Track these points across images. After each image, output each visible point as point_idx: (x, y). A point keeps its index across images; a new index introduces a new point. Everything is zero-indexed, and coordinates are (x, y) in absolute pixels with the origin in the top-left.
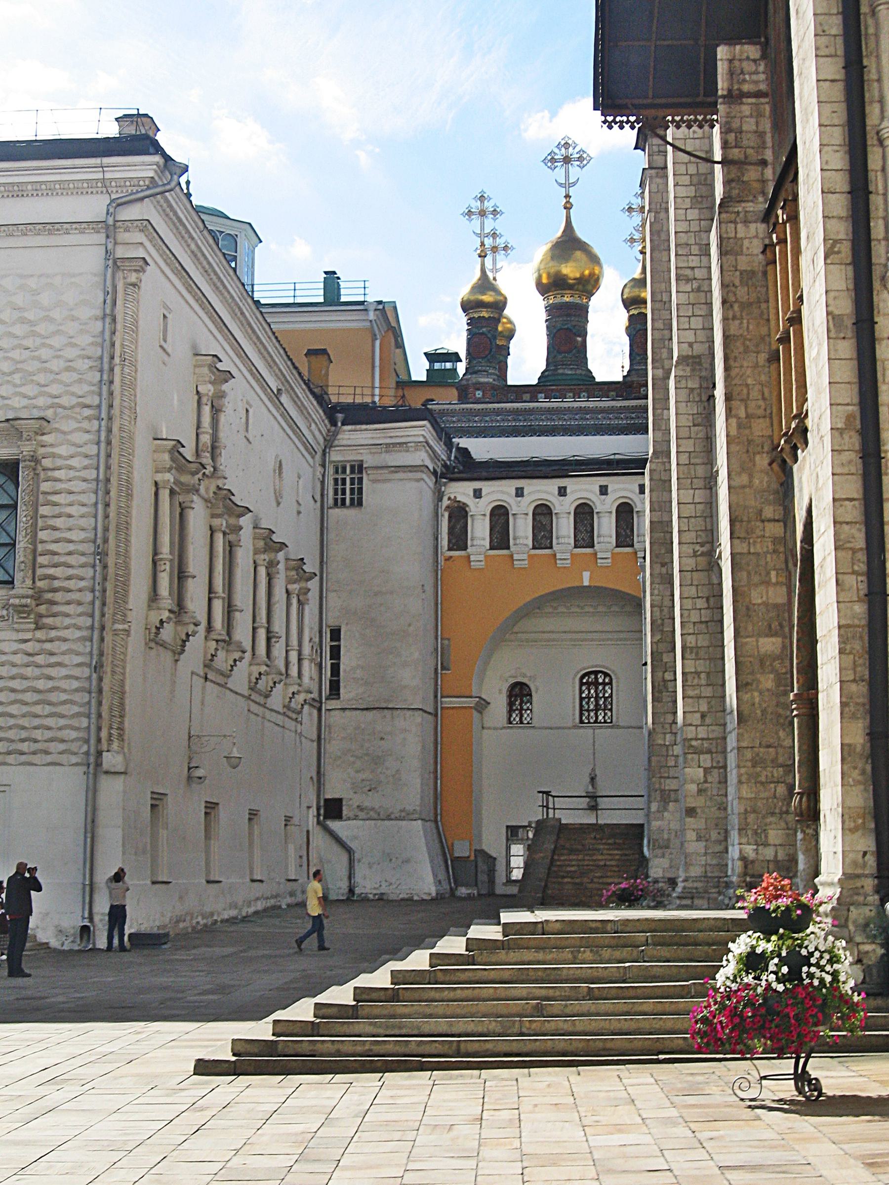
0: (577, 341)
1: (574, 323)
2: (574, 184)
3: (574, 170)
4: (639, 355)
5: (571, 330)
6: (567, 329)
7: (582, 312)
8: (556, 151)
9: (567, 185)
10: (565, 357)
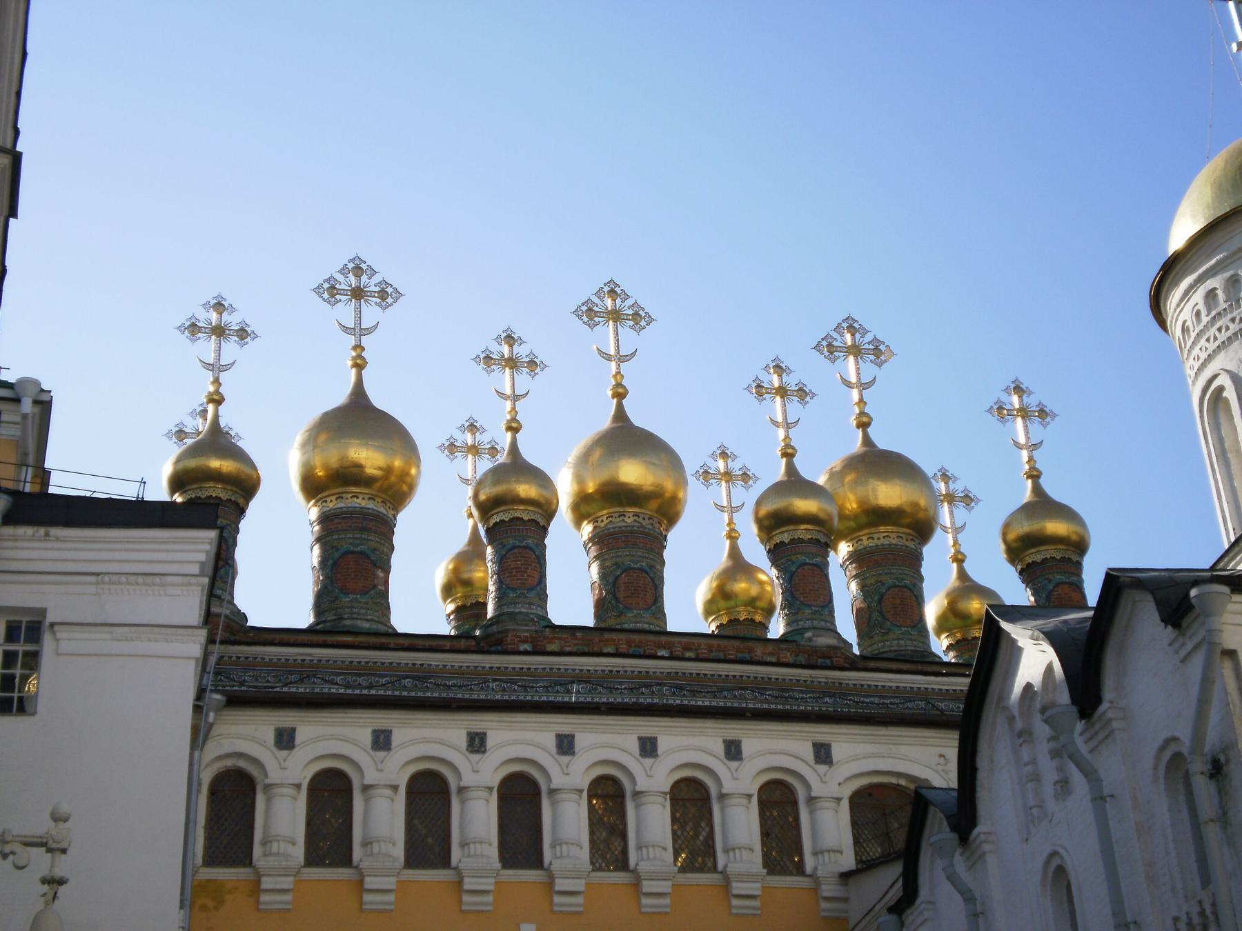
0: (378, 577)
1: (373, 545)
2: (369, 331)
3: (371, 313)
4: (514, 590)
5: (368, 557)
6: (361, 553)
7: (385, 528)
8: (340, 277)
9: (358, 331)
10: (356, 600)
